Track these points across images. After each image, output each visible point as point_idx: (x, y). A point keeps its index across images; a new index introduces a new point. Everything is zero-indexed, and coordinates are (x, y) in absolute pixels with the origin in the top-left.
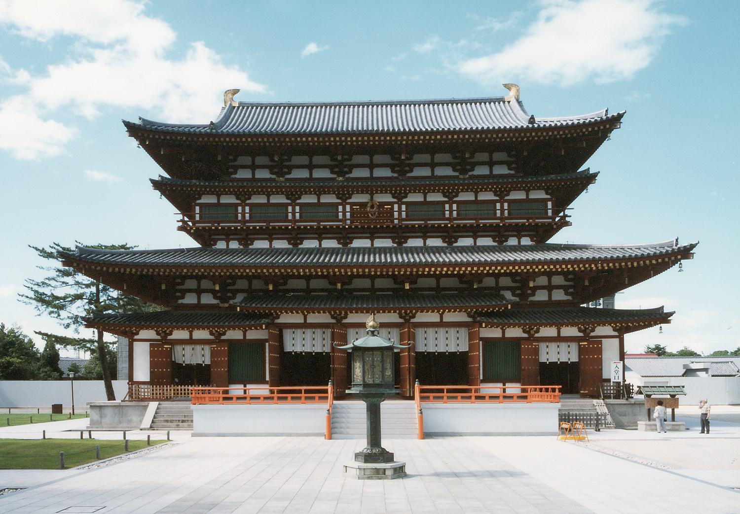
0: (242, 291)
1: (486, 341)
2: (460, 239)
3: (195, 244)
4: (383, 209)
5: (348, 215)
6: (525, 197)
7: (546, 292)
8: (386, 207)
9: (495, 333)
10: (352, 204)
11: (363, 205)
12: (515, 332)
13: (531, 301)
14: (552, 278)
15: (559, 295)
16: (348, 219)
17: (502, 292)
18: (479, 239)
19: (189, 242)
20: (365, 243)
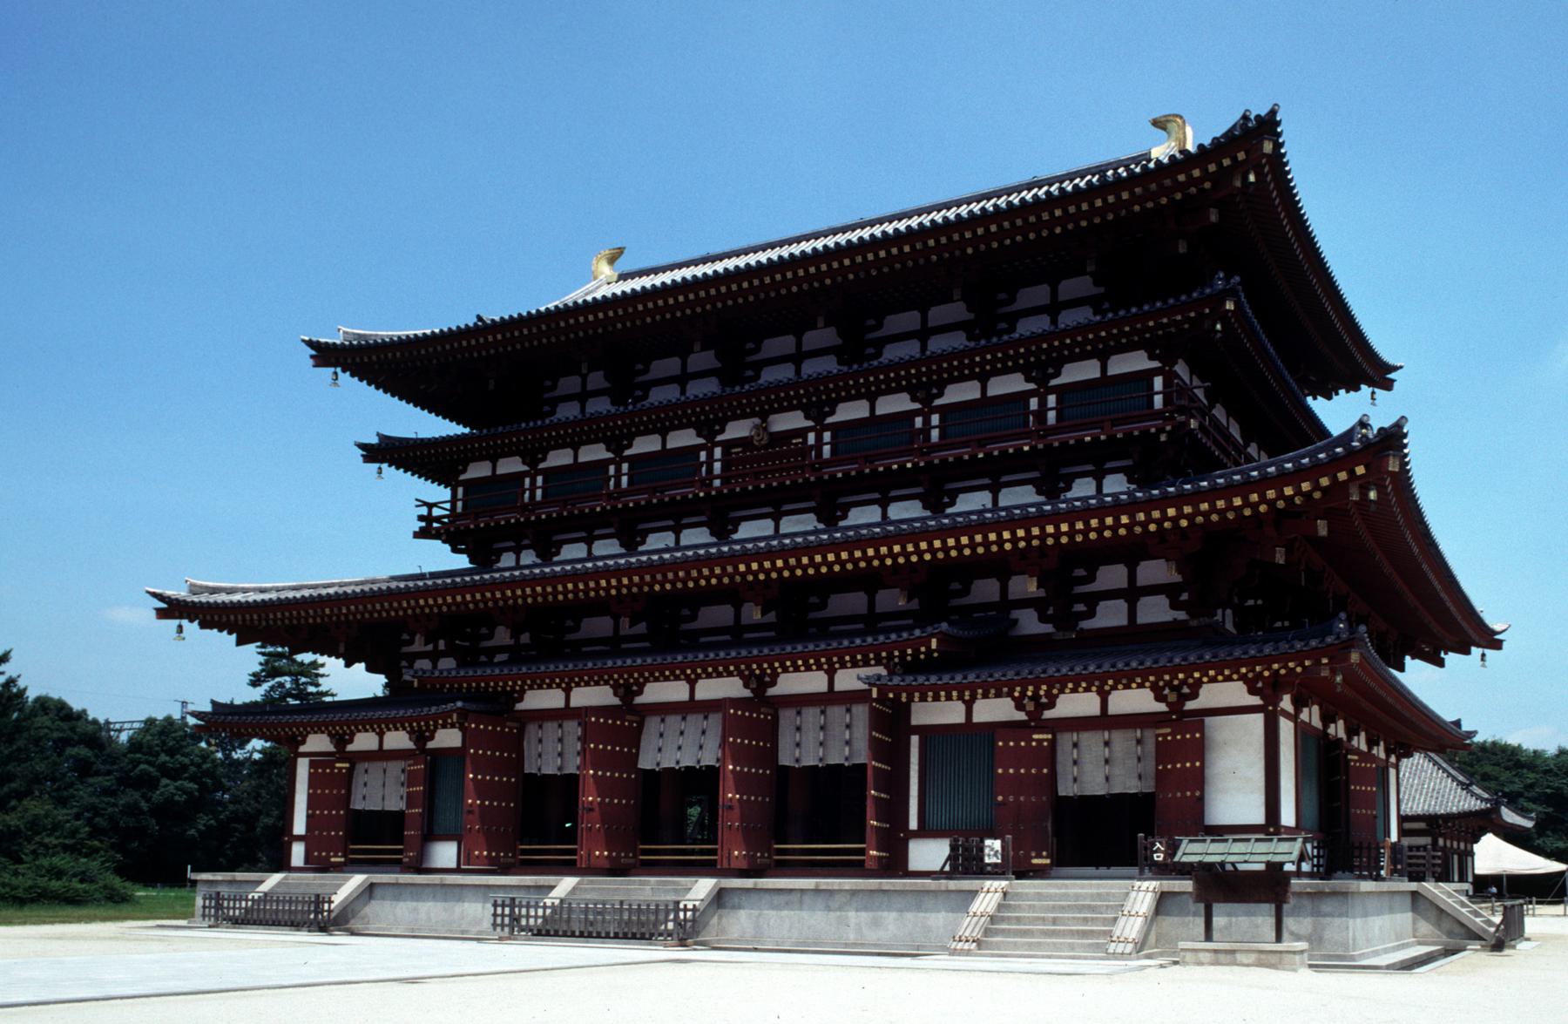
0: (502, 649)
1: (926, 732)
2: (961, 496)
3: (462, 562)
4: (788, 447)
5: (717, 466)
6: (977, 395)
7: (1121, 605)
8: (794, 441)
9: (950, 713)
10: (727, 445)
11: (744, 442)
12: (994, 710)
13: (1082, 629)
14: (1139, 569)
15: (1155, 611)
16: (717, 477)
17: (1015, 614)
18: (1004, 491)
19: (442, 558)
20: (763, 528)
